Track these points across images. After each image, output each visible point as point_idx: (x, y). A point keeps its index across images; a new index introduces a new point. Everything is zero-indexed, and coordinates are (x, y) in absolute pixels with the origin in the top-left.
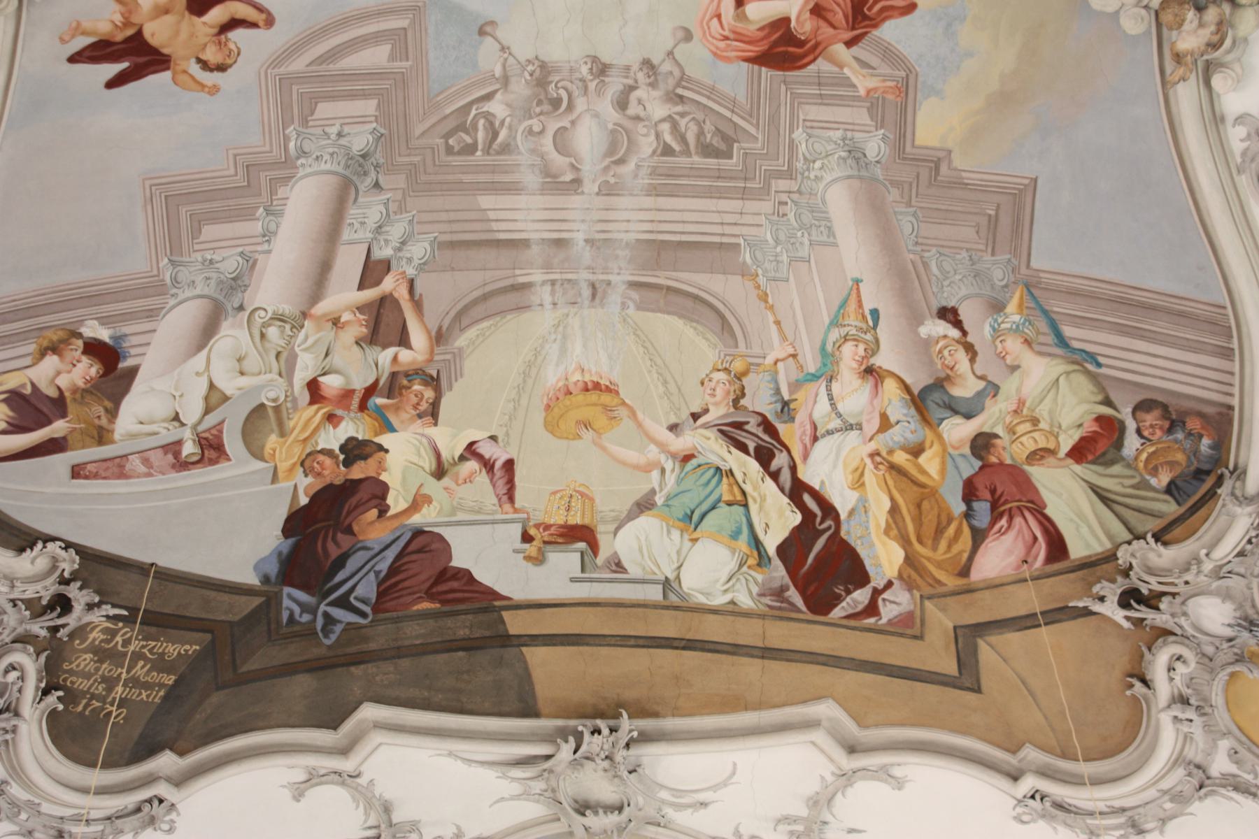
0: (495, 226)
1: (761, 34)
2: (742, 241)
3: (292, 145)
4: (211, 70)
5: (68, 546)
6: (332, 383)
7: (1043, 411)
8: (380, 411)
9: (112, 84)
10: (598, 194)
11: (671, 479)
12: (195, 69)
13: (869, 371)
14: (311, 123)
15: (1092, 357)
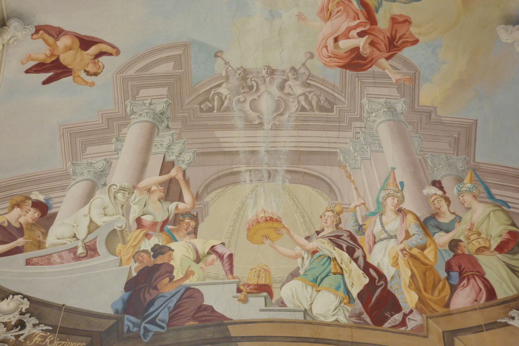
0: (223, 145)
1: (346, 55)
2: (339, 151)
3: (128, 109)
4: (91, 75)
5: (24, 297)
6: (147, 219)
7: (483, 229)
8: (170, 232)
9: (45, 83)
10: (271, 130)
11: (307, 263)
12: (83, 75)
13: (400, 211)
14: (137, 99)
15: (506, 203)
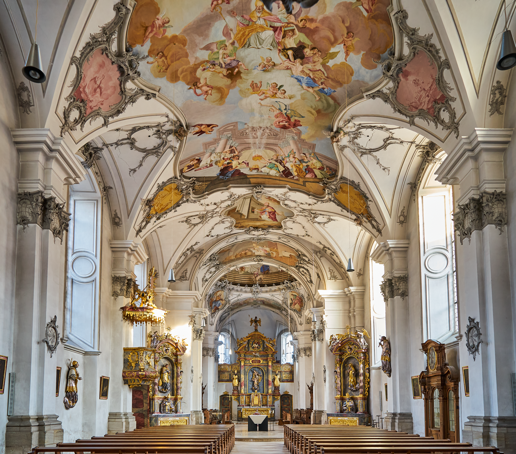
6: (226, 158)
